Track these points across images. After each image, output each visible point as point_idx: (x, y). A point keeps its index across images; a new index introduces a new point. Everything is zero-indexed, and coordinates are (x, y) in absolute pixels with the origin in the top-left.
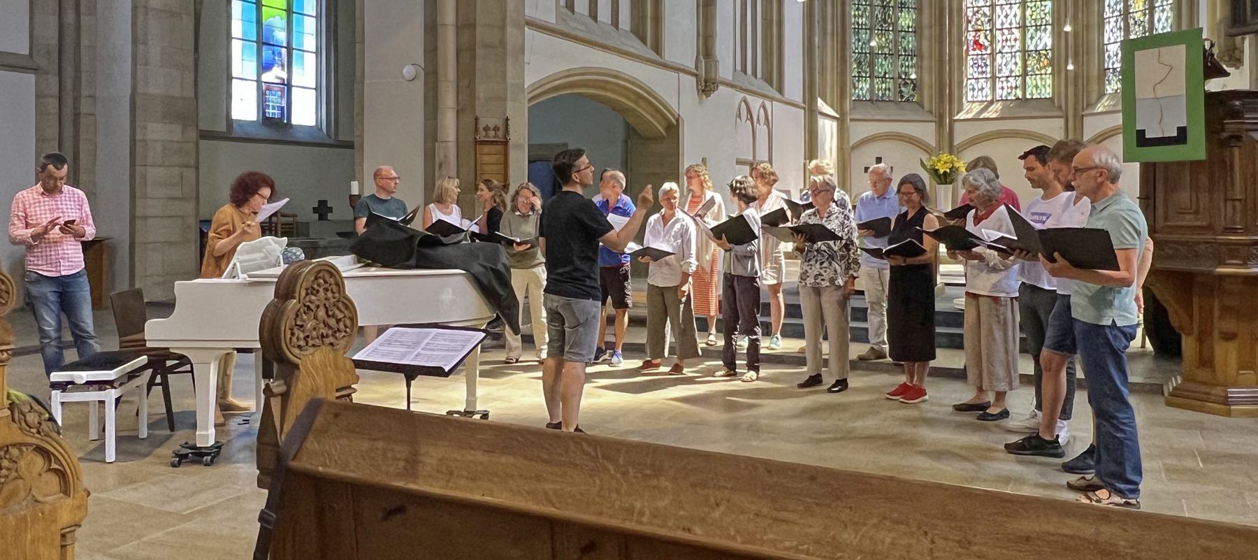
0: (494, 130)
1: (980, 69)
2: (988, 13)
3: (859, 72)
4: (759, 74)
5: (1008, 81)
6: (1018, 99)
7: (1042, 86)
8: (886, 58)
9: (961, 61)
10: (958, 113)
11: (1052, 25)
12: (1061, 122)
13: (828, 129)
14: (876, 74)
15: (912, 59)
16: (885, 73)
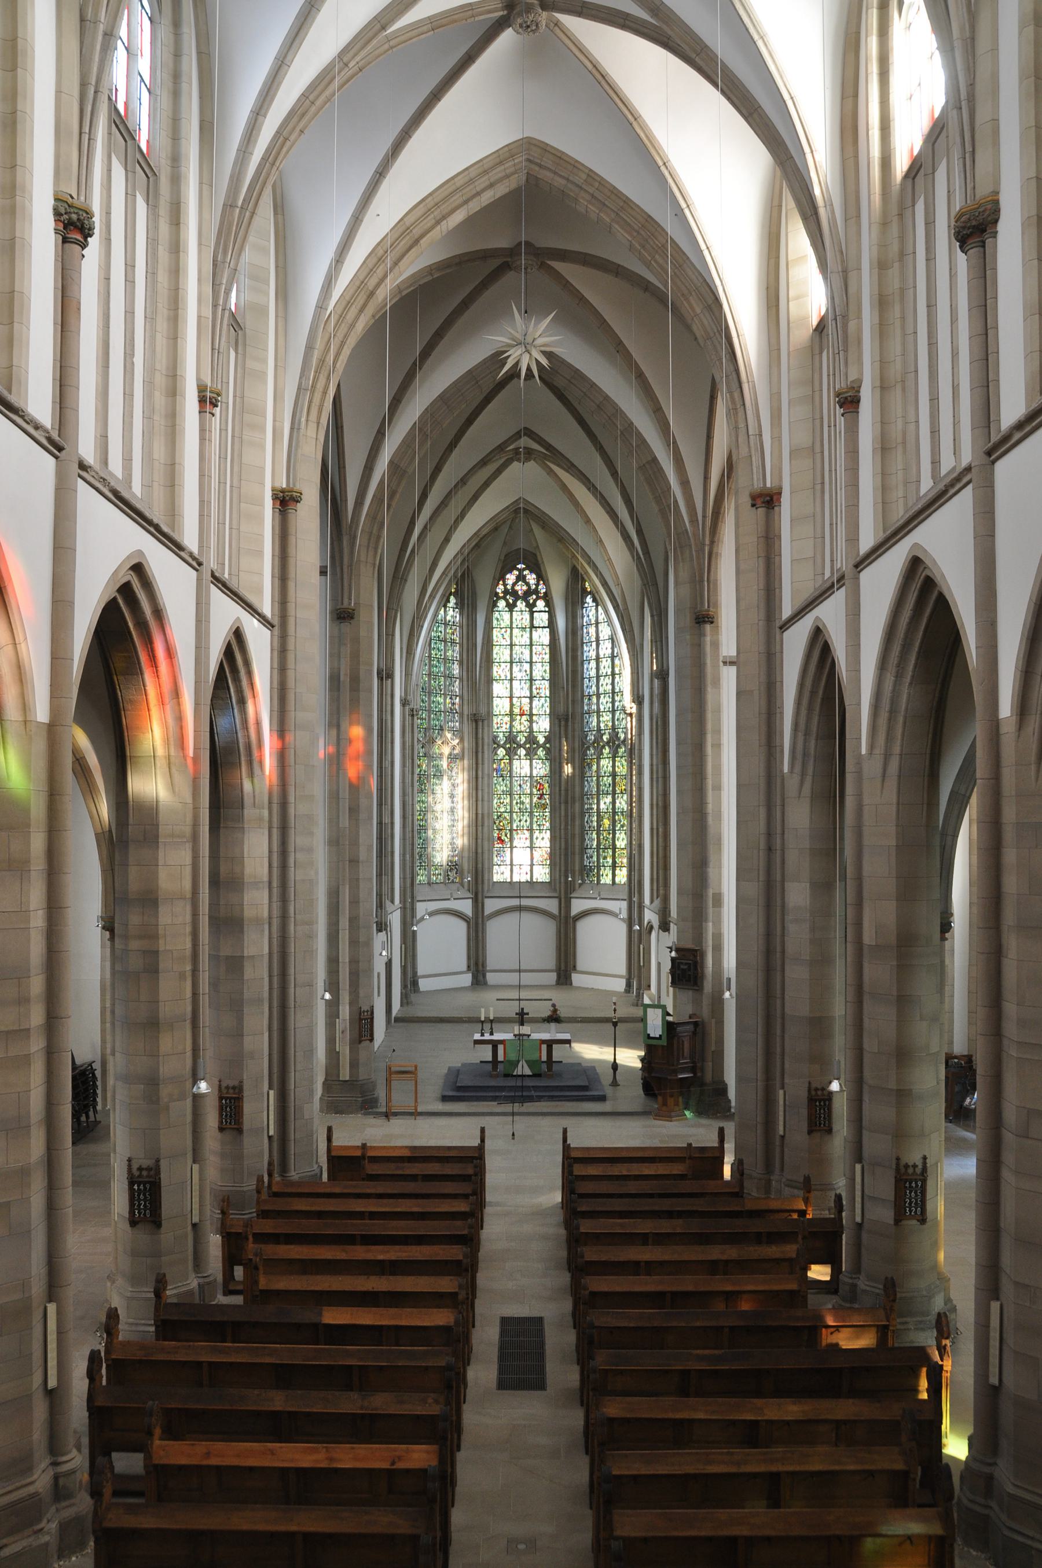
2: (508, 818)
6: (527, 882)
10: (488, 890)
11: (551, 830)
12: (555, 902)
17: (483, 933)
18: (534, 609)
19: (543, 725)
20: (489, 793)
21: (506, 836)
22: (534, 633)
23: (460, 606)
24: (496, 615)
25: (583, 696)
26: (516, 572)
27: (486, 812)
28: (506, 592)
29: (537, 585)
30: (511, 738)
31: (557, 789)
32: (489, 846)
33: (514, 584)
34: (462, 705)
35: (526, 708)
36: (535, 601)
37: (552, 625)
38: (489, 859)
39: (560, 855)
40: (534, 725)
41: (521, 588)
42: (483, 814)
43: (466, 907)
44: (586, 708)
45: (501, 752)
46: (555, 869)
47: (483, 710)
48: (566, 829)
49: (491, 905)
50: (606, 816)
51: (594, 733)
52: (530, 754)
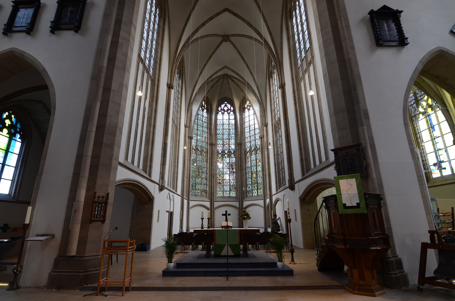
0: (102, 197)
1: (220, 189)
2: (222, 176)
3: (192, 188)
4: (169, 186)
5: (226, 192)
6: (228, 196)
7: (233, 194)
8: (199, 185)
9: (216, 186)
13: (185, 201)
14: (196, 189)
15: (205, 185)
16: (199, 189)
17: (213, 214)
18: (230, 114)
19: (233, 147)
20: (216, 168)
21: (221, 181)
22: (230, 121)
23: (207, 112)
24: (218, 116)
25: (245, 138)
26: (224, 104)
27: (215, 173)
28: (221, 110)
29: (231, 108)
30: (223, 151)
31: (238, 166)
32: (216, 185)
33: (224, 108)
34: (208, 141)
35: (227, 142)
36: (230, 112)
37: (235, 119)
38: (216, 189)
39: (239, 187)
40: (230, 147)
41: (226, 109)
42: (214, 174)
43: (208, 204)
44: (246, 141)
45: (220, 155)
46: (238, 192)
47: (214, 142)
48: (241, 178)
49: (216, 204)
50: (254, 173)
51: (249, 148)
52: (229, 156)
